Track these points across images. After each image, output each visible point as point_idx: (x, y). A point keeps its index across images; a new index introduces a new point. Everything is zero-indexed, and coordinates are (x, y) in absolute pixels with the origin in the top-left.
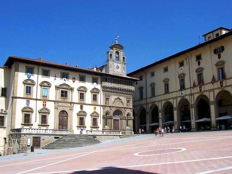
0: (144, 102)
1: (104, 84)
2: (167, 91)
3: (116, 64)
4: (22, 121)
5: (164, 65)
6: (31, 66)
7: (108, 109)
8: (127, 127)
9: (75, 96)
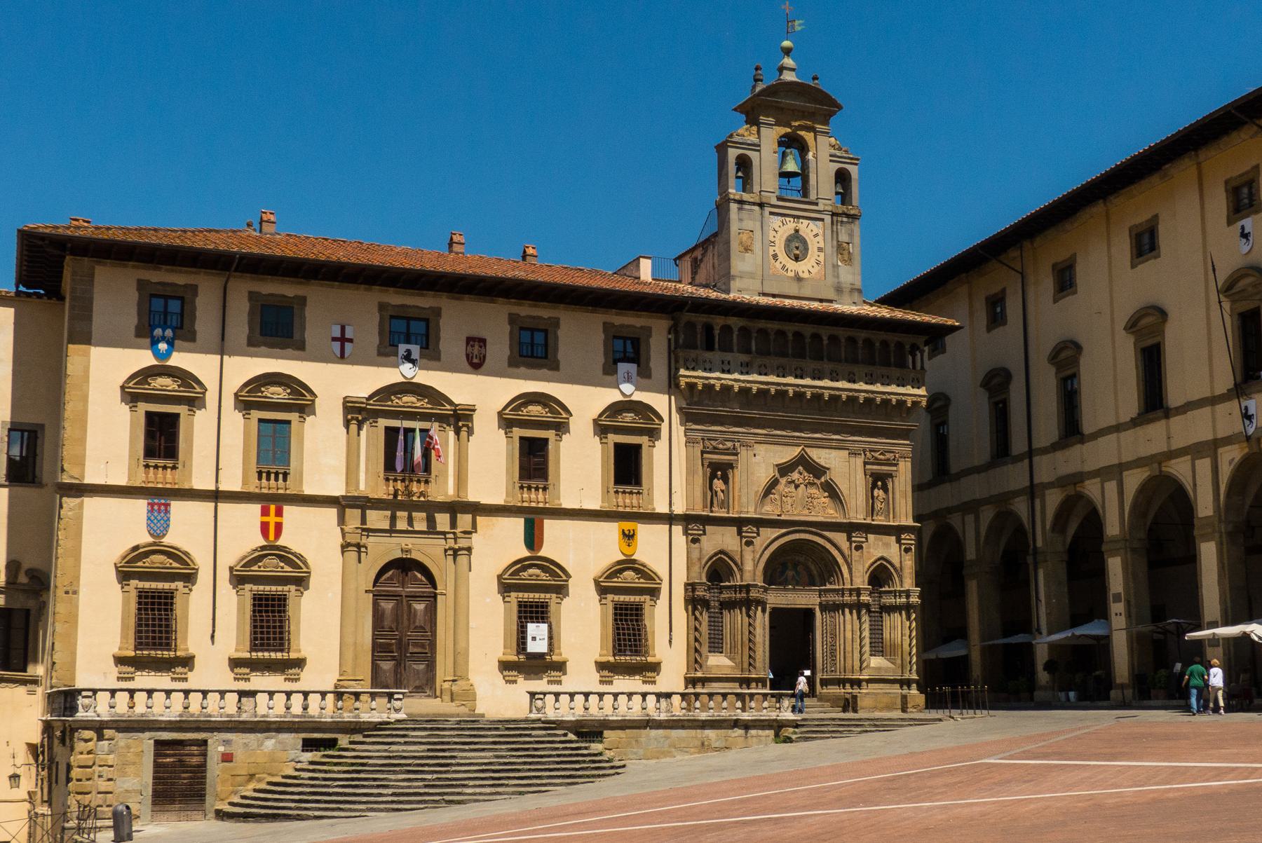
0: (1014, 477)
1: (687, 373)
2: (1154, 402)
3: (781, 229)
4: (124, 636)
5: (1132, 209)
6: (172, 284)
7: (722, 539)
8: (876, 662)
9: (482, 465)
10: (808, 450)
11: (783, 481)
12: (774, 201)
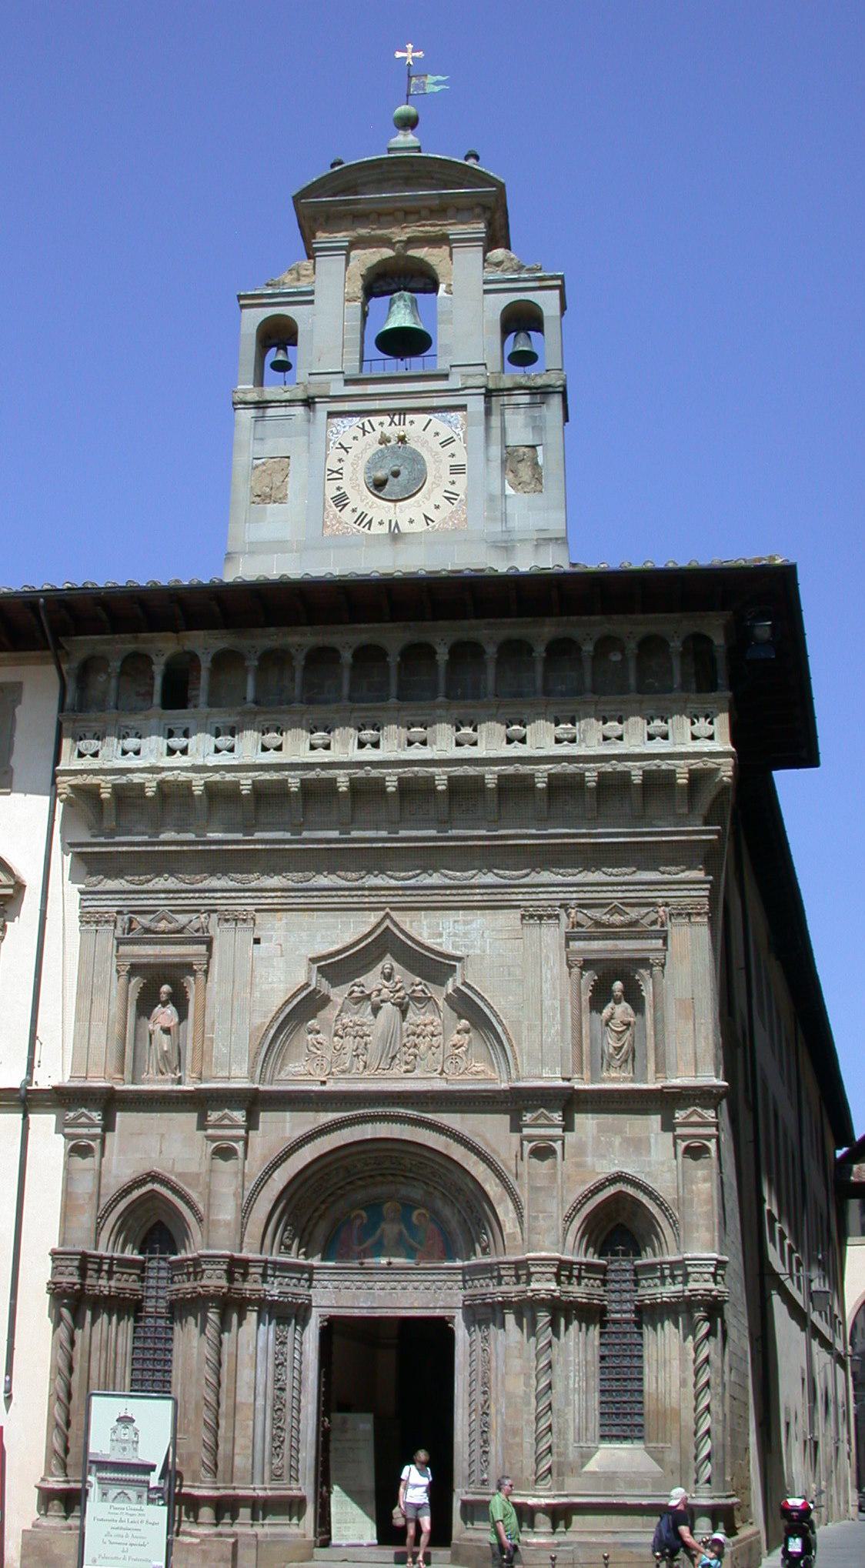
7: (164, 1146)
10: (393, 914)
11: (338, 995)
12: (338, 388)
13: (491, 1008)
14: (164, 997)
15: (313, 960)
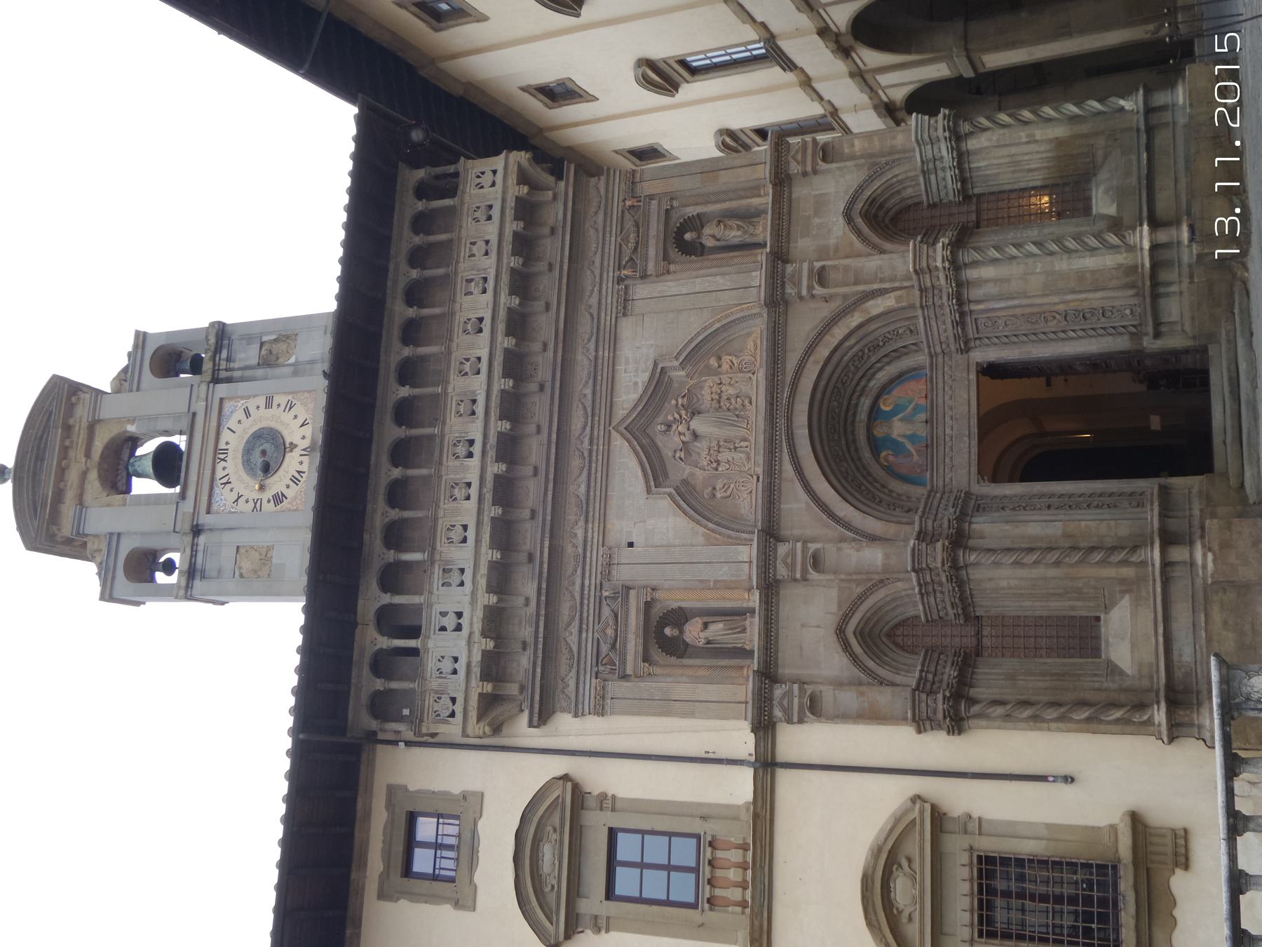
11: (680, 471)
12: (188, 507)
13: (698, 334)
14: (676, 632)
15: (649, 491)
